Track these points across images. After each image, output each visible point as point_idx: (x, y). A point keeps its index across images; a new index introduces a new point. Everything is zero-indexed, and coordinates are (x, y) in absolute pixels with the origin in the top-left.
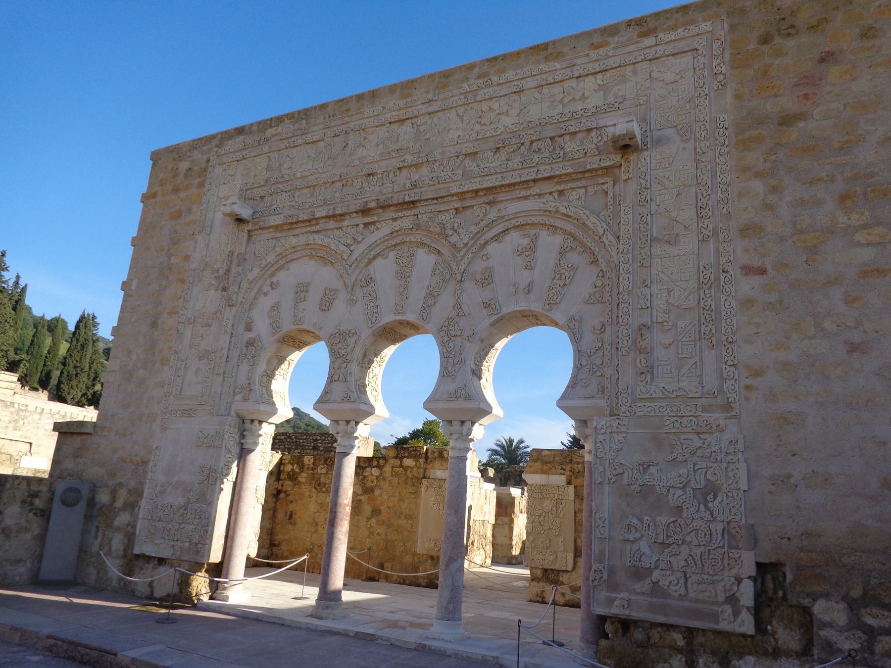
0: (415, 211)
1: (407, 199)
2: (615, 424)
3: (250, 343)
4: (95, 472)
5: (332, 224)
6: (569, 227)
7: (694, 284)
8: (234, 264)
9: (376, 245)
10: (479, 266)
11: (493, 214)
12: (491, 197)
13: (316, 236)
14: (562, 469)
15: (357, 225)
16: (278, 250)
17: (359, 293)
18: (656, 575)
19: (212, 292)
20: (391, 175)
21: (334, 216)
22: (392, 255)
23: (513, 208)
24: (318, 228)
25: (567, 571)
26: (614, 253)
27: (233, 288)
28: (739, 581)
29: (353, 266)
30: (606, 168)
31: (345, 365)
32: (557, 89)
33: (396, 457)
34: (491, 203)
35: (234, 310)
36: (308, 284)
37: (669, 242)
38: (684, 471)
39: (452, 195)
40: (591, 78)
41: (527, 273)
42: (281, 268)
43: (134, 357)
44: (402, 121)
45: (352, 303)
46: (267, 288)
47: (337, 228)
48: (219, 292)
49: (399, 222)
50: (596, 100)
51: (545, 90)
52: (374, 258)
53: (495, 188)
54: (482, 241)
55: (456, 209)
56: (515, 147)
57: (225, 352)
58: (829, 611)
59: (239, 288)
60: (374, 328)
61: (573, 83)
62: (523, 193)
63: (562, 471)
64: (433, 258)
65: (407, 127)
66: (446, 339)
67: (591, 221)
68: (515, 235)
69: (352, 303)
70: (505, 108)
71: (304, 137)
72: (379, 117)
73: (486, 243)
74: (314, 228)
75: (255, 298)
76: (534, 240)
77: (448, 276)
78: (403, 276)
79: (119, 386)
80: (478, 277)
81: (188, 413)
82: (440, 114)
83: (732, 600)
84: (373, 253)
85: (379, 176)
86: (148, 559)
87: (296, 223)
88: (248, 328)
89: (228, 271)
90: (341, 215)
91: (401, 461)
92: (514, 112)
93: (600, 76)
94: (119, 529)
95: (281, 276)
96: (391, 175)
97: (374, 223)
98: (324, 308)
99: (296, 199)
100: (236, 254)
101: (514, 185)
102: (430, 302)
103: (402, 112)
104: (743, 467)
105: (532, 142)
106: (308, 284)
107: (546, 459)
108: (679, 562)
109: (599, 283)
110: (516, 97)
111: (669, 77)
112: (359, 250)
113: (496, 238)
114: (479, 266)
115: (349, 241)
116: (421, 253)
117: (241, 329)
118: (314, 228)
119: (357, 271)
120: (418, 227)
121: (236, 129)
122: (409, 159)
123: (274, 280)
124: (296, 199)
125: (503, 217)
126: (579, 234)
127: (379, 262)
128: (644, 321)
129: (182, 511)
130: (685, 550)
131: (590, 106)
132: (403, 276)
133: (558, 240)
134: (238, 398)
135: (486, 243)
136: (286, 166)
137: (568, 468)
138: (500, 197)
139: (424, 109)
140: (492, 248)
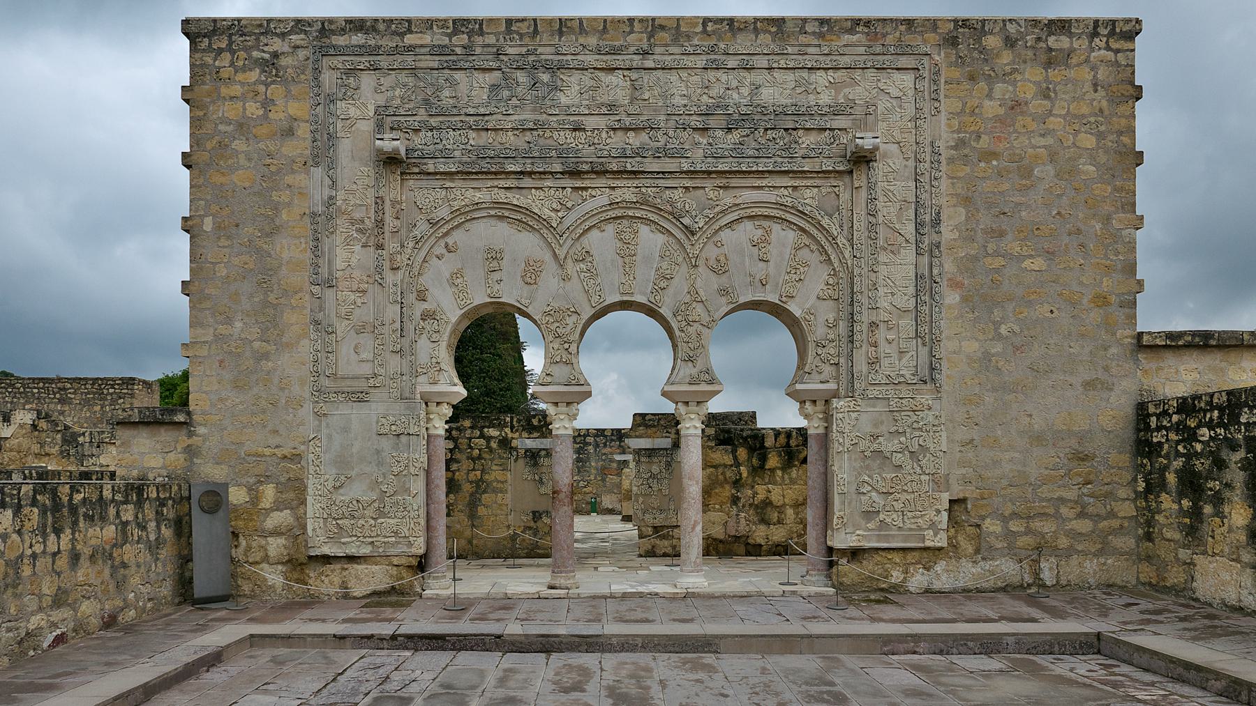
0: (637, 182)
1: (629, 168)
2: (852, 404)
3: (425, 316)
4: (212, 472)
5: (527, 182)
6: (802, 224)
7: (912, 290)
8: (387, 215)
9: (589, 215)
10: (712, 252)
11: (728, 199)
12: (724, 181)
13: (509, 195)
16: (456, 205)
17: (571, 268)
18: (882, 516)
19: (357, 248)
20: (604, 135)
21: (530, 174)
22: (610, 229)
23: (749, 196)
24: (508, 183)
26: (847, 255)
27: (392, 245)
28: (938, 511)
29: (565, 236)
30: (837, 172)
31: (566, 346)
32: (790, 76)
34: (725, 188)
35: (400, 274)
37: (892, 252)
38: (903, 439)
39: (681, 172)
40: (822, 73)
41: (762, 264)
42: (457, 227)
43: (238, 325)
44: (612, 70)
45: (566, 279)
46: (439, 249)
48: (372, 249)
49: (619, 192)
50: (825, 99)
51: (776, 74)
52: (590, 228)
53: (730, 172)
55: (686, 188)
56: (748, 131)
57: (398, 325)
58: (992, 526)
59: (403, 246)
61: (805, 74)
62: (758, 183)
64: (660, 239)
65: (614, 79)
66: (684, 323)
67: (825, 222)
68: (748, 225)
69: (566, 279)
70: (734, 84)
71: (471, 58)
72: (579, 57)
74: (502, 183)
75: (424, 261)
76: (768, 232)
77: (680, 259)
78: (627, 254)
79: (221, 362)
80: (712, 262)
81: (360, 397)
82: (659, 73)
83: (933, 525)
84: (588, 224)
85: (589, 133)
86: (326, 559)
87: (476, 173)
88: (422, 297)
89: (380, 223)
90: (540, 173)
92: (745, 91)
93: (830, 72)
94: (276, 533)
95: (457, 237)
96: (604, 135)
97: (585, 189)
99: (471, 142)
100: (388, 204)
101: (750, 172)
102: (663, 285)
103: (608, 57)
104: (944, 434)
105: (766, 130)
108: (898, 506)
109: (831, 282)
110: (746, 74)
111: (895, 92)
113: (729, 225)
114: (712, 252)
115: (554, 206)
116: (644, 230)
117: (412, 297)
118: (502, 183)
119: (569, 242)
120: (645, 202)
121: (349, 21)
122: (628, 121)
123: (450, 240)
124: (471, 142)
126: (814, 232)
127: (595, 233)
128: (874, 319)
129: (376, 505)
130: (904, 496)
131: (821, 102)
132: (627, 254)
133: (791, 235)
134: (421, 379)
136: (446, 93)
138: (734, 182)
139: (637, 61)
140: (725, 235)
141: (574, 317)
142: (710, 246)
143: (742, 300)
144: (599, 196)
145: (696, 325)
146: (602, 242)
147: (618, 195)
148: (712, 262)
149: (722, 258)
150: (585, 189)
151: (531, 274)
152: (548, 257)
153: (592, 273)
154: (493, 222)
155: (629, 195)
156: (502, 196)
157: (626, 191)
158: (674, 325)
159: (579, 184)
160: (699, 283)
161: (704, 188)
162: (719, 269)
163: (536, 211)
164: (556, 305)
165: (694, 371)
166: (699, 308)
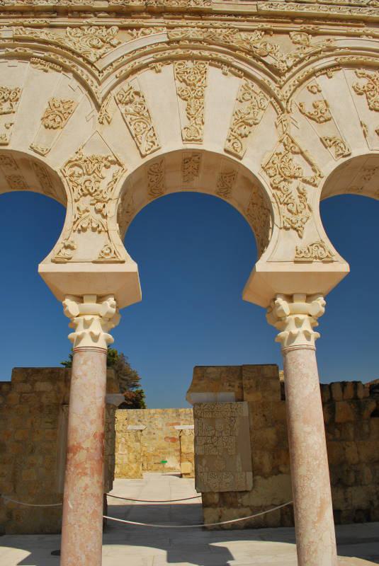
14: (230, 385)
15: (108, 27)
22: (168, 70)
25: (246, 491)
29: (105, 73)
31: (99, 206)
33: (25, 382)
36: (17, 91)
45: (105, 121)
47: (72, 27)
54: (309, 69)
60: (148, 158)
63: (230, 388)
66: (278, 178)
68: (349, 73)
73: (314, 74)
78: (192, 95)
91: (33, 385)
98: (51, 123)
102: (243, 131)
106: (17, 91)
107: (212, 376)
112: (113, 56)
113: (325, 70)
115: (95, 42)
116: (214, 73)
119: (112, 80)
125: (334, 49)
127: (147, 74)
132: (192, 95)
135: (314, 74)
137: (237, 384)
138: (323, 28)
140: (321, 81)
141: (115, 168)
142: (303, 91)
143: (356, 153)
144: (155, 34)
145: (296, 183)
146: (158, 86)
147: (177, 34)
148: (308, 109)
149: (322, 105)
150: (138, 28)
151: (56, 116)
152: (82, 95)
153: (143, 116)
154: (15, 62)
155: (193, 33)
156: (27, 33)
157: (191, 29)
158: (265, 181)
159: (128, 22)
160: (293, 131)
161: (287, 32)
162: (319, 117)
163: (70, 45)
164: (86, 153)
165: (302, 244)
166: (298, 160)
